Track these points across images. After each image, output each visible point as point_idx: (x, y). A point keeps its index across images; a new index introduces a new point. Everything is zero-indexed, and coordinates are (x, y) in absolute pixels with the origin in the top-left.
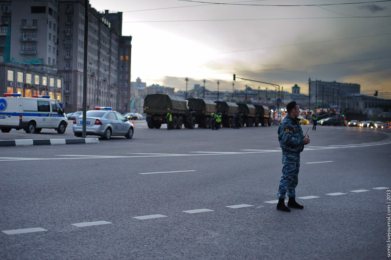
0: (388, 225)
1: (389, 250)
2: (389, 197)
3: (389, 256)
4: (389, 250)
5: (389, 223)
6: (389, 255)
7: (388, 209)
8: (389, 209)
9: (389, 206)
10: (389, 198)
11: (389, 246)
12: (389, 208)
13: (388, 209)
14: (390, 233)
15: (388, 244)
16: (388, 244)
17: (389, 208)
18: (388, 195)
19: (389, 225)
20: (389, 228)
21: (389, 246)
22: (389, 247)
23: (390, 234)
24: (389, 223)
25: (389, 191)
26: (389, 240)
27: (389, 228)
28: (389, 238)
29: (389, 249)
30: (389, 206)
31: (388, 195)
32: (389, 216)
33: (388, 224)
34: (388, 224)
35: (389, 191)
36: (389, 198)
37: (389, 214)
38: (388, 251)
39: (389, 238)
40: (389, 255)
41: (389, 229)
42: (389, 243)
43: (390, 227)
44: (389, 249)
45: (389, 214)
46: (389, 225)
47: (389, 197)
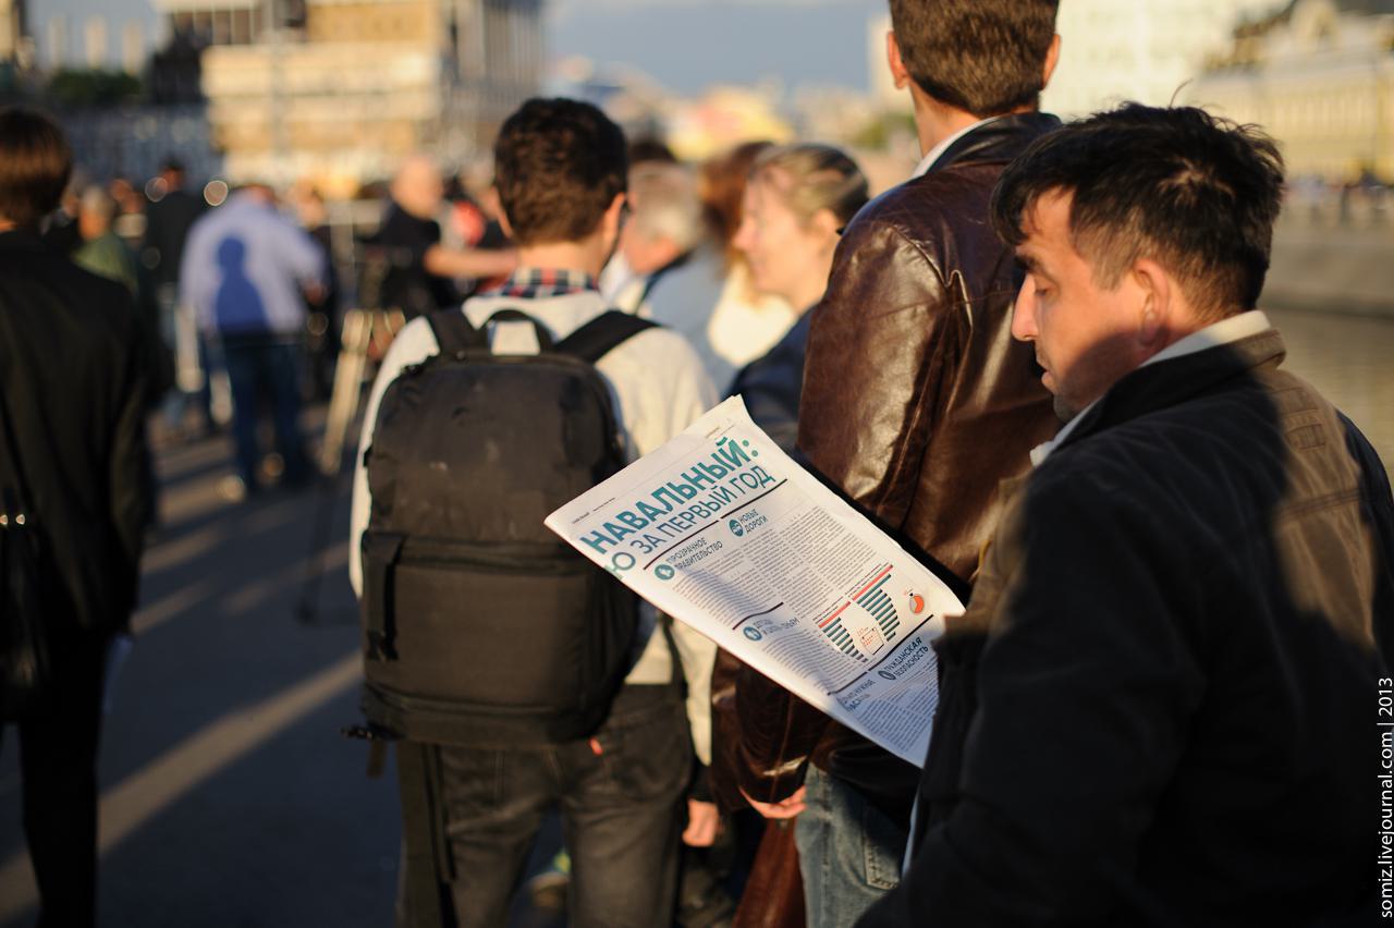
0: (1385, 804)
1: (1386, 893)
2: (1382, 702)
3: (1387, 913)
4: (1386, 893)
5: (1386, 795)
6: (1386, 911)
7: (1384, 746)
8: (1386, 748)
9: (1386, 737)
10: (1388, 708)
11: (1386, 877)
13: (1384, 746)
15: (1384, 871)
16: (1384, 871)
18: (1384, 695)
19: (1387, 801)
20: (1388, 813)
21: (1386, 877)
22: (1387, 882)
24: (1386, 795)
25: (1388, 682)
27: (1388, 813)
28: (1386, 850)
29: (1386, 887)
30: (1386, 737)
31: (1384, 695)
32: (1386, 772)
33: (1384, 798)
34: (1384, 798)
35: (1388, 682)
36: (1388, 708)
37: (1387, 763)
38: (1384, 896)
39: (1386, 850)
40: (1386, 911)
41: (1386, 819)
42: (1386, 867)
43: (1390, 810)
44: (1386, 887)
45: (1387, 763)
46: (1387, 801)
47: (1388, 702)
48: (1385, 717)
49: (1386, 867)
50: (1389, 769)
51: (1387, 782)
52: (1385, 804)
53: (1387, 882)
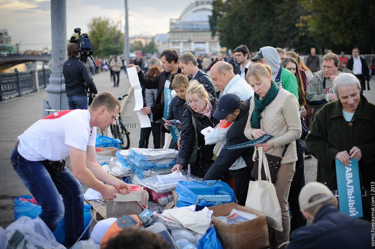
0: (372, 216)
1: (373, 240)
2: (372, 188)
3: (373, 245)
4: (373, 240)
5: (373, 213)
6: (373, 245)
7: (372, 200)
8: (373, 201)
9: (373, 198)
10: (373, 190)
11: (373, 235)
12: (373, 199)
14: (374, 223)
15: (372, 234)
16: (372, 234)
17: (373, 199)
18: (372, 186)
19: (373, 215)
20: (373, 218)
21: (373, 235)
22: (373, 237)
23: (374, 224)
24: (373, 213)
25: (373, 183)
26: (373, 230)
27: (373, 218)
28: (373, 228)
29: (373, 238)
30: (373, 198)
31: (372, 186)
32: (373, 207)
33: (372, 214)
34: (372, 214)
35: (373, 183)
36: (373, 190)
38: (372, 240)
39: (373, 228)
40: (373, 245)
42: (373, 233)
44: (373, 238)
45: (373, 205)
46: (373, 215)
47: (373, 188)
48: (373, 192)
49: (373, 233)
50: (374, 206)
51: (373, 210)
52: (372, 216)
53: (373, 237)
